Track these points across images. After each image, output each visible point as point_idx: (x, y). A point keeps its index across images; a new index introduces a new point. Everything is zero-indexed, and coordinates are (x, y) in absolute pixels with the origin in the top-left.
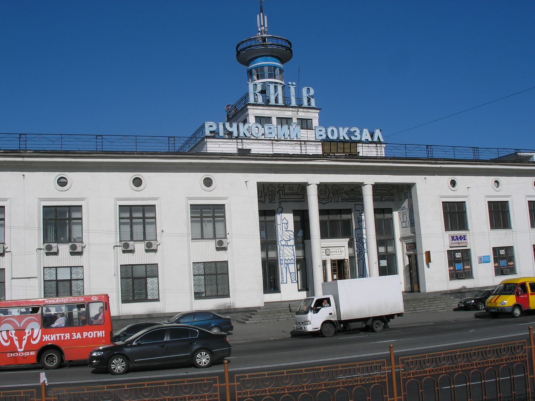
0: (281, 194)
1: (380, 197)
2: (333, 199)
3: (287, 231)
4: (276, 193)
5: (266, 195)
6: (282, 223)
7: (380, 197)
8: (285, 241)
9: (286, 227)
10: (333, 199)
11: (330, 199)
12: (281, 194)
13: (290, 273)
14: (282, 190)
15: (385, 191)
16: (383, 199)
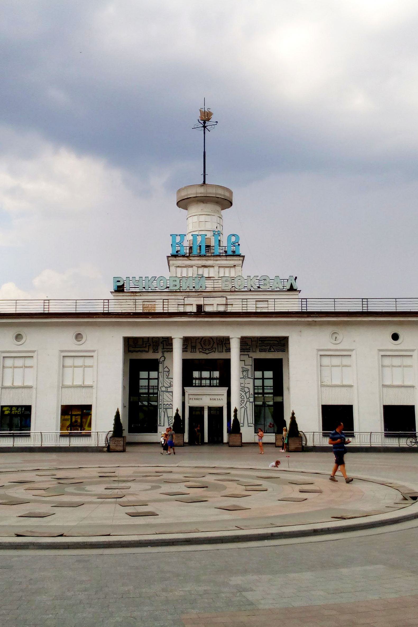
0: (165, 345)
1: (269, 347)
2: (217, 349)
3: (168, 378)
4: (160, 343)
5: (150, 345)
6: (164, 371)
7: (269, 347)
8: (166, 387)
9: (168, 375)
10: (217, 349)
11: (214, 350)
12: (165, 345)
13: (168, 417)
14: (166, 341)
15: (276, 342)
16: (272, 350)
